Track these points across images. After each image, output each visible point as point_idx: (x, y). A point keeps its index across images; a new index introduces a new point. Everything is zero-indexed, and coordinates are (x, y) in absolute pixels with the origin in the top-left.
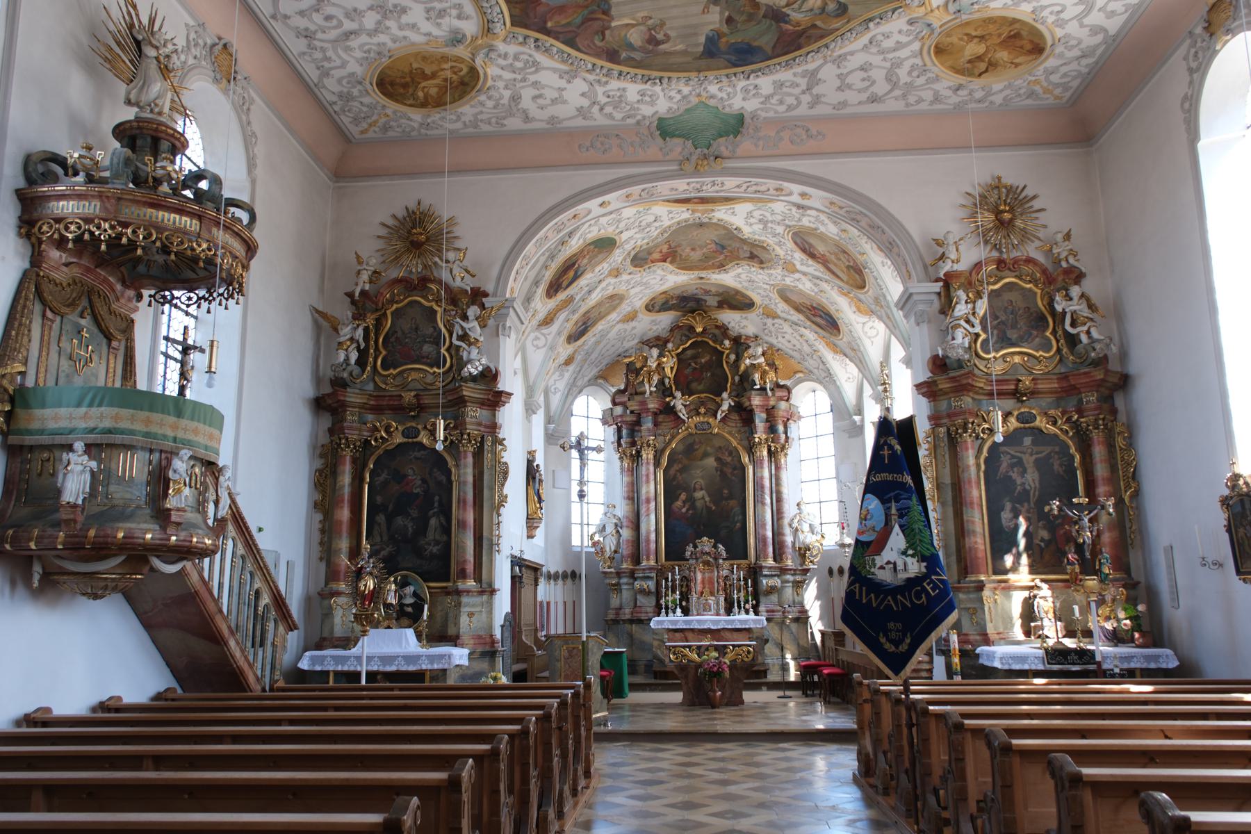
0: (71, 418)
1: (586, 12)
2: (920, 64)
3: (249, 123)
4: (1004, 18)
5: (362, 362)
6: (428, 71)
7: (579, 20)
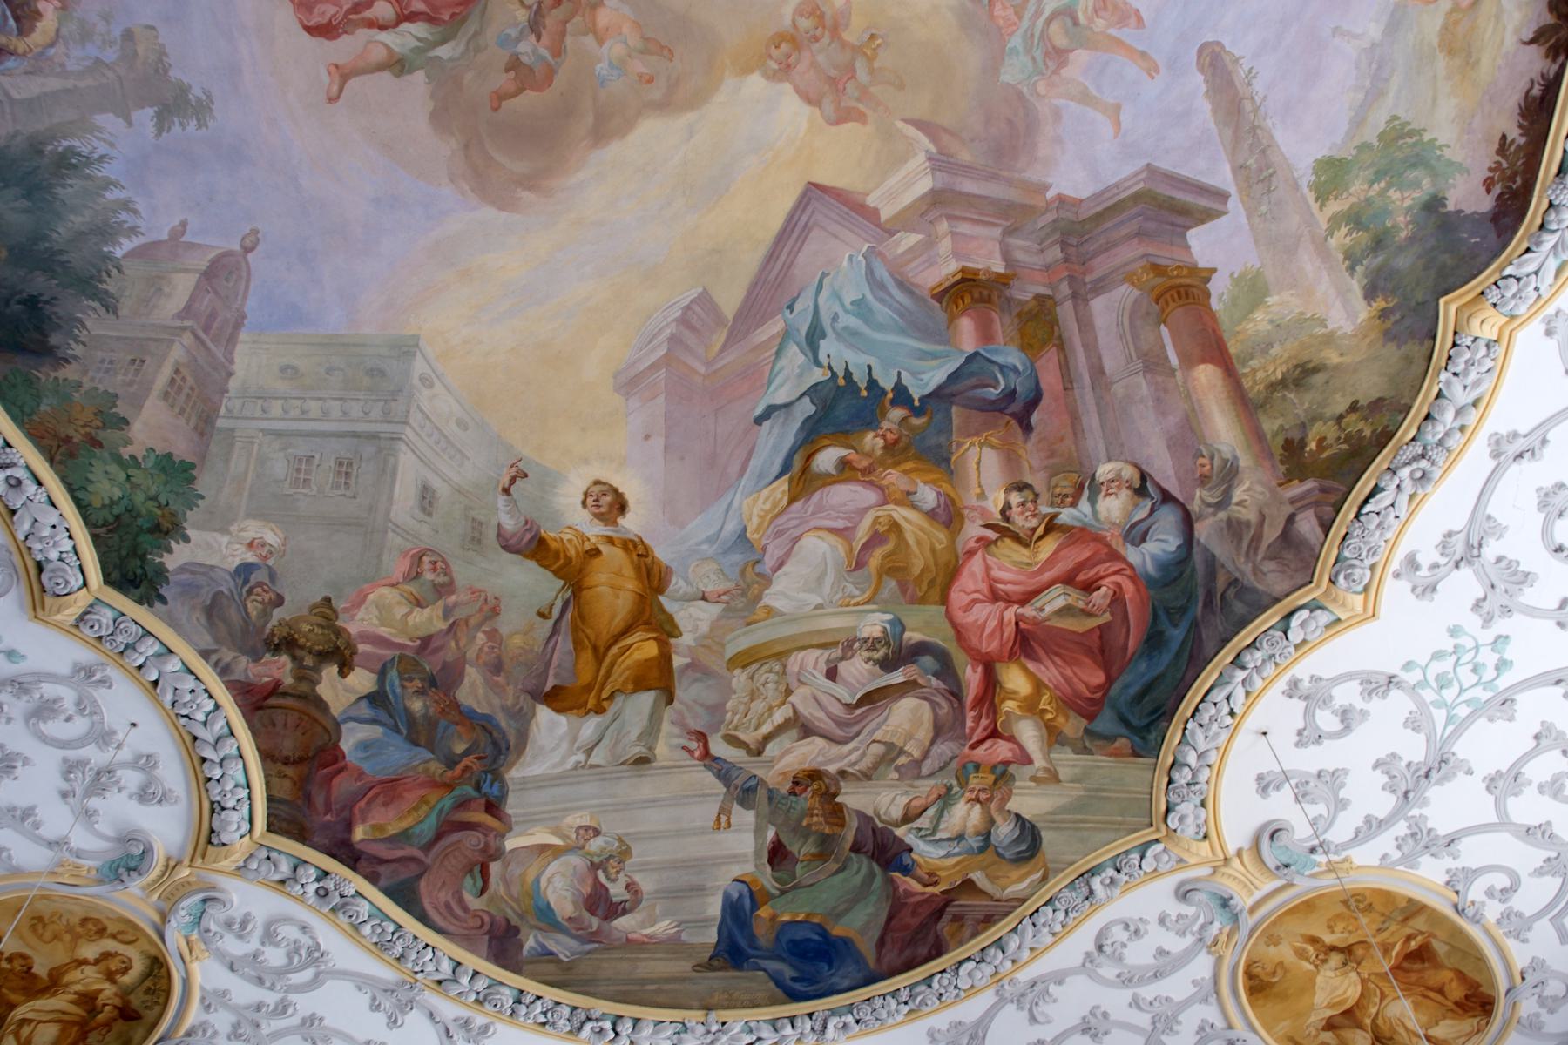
1: (448, 802)
2: (1219, 1024)
4: (1387, 896)
6: (41, 969)
7: (429, 826)
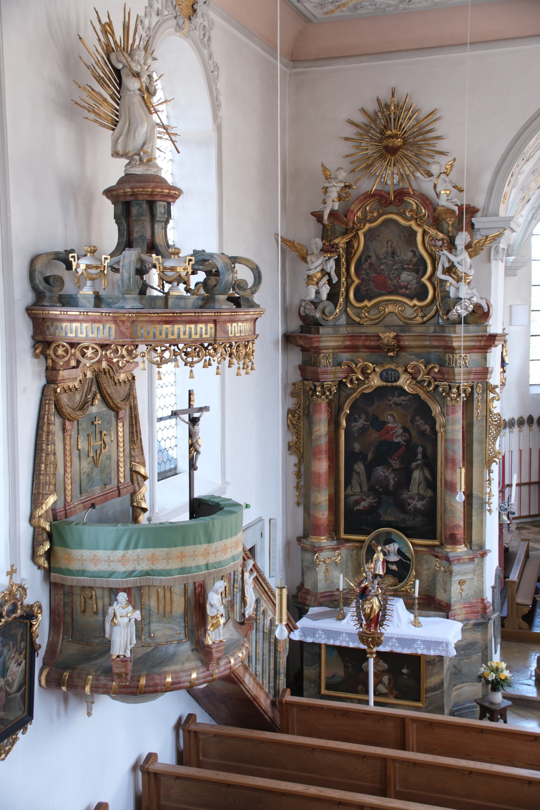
0: (109, 561)
3: (210, 57)
5: (333, 297)
